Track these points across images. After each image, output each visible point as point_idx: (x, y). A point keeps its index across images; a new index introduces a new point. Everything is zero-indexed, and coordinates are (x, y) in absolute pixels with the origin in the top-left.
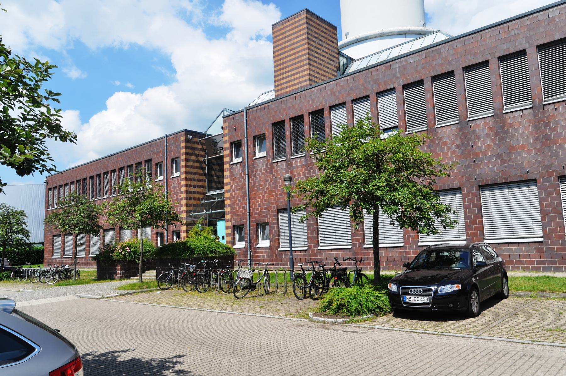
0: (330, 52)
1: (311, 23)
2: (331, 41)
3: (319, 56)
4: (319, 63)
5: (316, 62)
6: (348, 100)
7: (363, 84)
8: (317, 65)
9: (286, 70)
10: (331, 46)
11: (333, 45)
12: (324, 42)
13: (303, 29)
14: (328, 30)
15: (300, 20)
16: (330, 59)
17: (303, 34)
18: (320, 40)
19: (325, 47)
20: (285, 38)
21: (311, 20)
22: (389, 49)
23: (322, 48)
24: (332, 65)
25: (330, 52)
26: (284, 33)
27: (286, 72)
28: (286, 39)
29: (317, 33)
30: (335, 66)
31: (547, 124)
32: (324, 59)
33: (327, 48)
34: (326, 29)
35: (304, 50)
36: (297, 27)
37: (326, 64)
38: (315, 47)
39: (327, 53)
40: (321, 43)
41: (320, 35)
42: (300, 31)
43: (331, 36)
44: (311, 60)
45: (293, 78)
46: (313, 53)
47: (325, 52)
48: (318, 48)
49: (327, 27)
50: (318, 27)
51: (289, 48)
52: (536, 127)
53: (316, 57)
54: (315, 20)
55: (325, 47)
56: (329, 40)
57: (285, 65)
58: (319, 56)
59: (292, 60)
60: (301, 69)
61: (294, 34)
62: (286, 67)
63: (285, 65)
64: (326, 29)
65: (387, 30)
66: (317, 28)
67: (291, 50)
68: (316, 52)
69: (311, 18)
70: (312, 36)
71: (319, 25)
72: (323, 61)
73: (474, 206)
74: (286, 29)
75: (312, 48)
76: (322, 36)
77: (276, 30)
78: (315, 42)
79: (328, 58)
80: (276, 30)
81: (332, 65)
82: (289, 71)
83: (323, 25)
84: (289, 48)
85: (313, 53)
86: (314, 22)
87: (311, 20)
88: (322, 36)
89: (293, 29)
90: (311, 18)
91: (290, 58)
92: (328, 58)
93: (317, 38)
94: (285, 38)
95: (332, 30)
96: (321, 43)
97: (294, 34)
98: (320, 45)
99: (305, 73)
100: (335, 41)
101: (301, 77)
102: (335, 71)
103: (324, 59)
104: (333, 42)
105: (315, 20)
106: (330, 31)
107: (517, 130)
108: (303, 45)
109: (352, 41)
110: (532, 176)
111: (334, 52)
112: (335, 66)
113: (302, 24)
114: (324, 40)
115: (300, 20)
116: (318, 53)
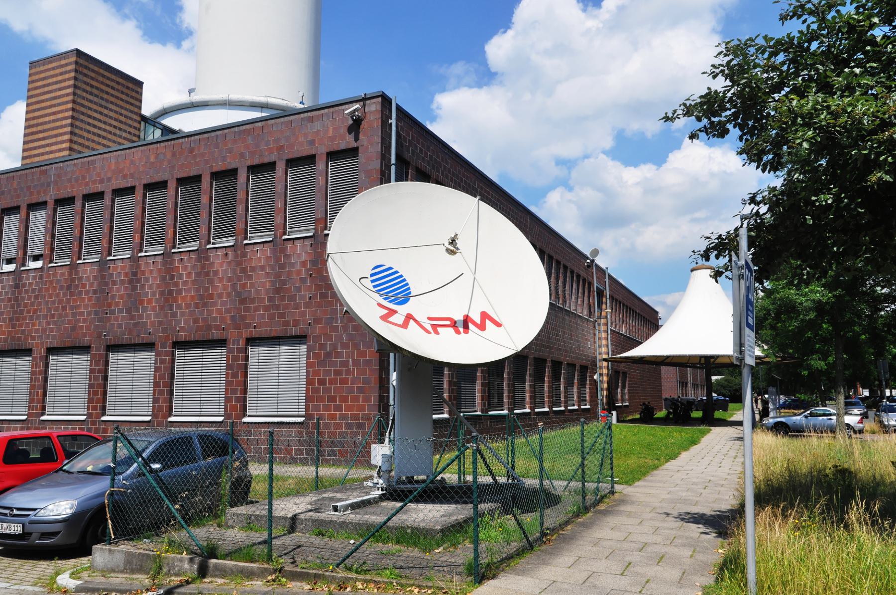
0: (122, 118)
1: (85, 71)
2: (127, 102)
3: (96, 123)
7: (15, 190)
8: (90, 136)
9: (41, 135)
10: (127, 110)
11: (132, 108)
12: (112, 103)
13: (69, 79)
14: (123, 85)
15: (66, 65)
16: (120, 129)
17: (69, 87)
18: (102, 98)
19: (111, 110)
20: (44, 86)
21: (86, 67)
23: (106, 112)
25: (122, 118)
26: (44, 79)
27: (39, 140)
28: (46, 89)
29: (97, 88)
31: (172, 277)
32: (108, 128)
33: (116, 112)
34: (118, 83)
35: (67, 110)
36: (61, 74)
37: (110, 136)
38: (90, 109)
39: (116, 120)
40: (103, 103)
41: (102, 91)
42: (65, 80)
43: (127, 95)
44: (77, 127)
45: (47, 149)
47: (111, 118)
48: (96, 111)
49: (121, 80)
50: (101, 79)
51: (48, 103)
52: (163, 278)
53: (89, 124)
54: (96, 69)
55: (111, 110)
56: (122, 100)
57: (40, 128)
58: (96, 123)
59: (49, 122)
60: (60, 139)
61: (56, 83)
62: (41, 132)
63: (40, 128)
64: (118, 83)
65: (235, 97)
66: (97, 81)
67: (51, 107)
68: (89, 116)
69: (86, 63)
70: (84, 90)
71: (103, 76)
72: (105, 130)
73: (100, 371)
74: (48, 74)
75: (82, 109)
76: (107, 93)
77: (33, 71)
78: (91, 101)
79: (115, 127)
80: (33, 71)
82: (44, 139)
83: (113, 77)
84: (48, 103)
85: (82, 117)
86: (93, 71)
87: (86, 67)
88: (107, 93)
89: (56, 75)
90: (86, 63)
91: (47, 119)
92: (115, 127)
93: (96, 96)
94: (44, 86)
95: (130, 85)
96: (103, 103)
97: (56, 83)
98: (101, 106)
99: (64, 146)
100: (137, 103)
101: (60, 149)
103: (108, 128)
104: (132, 104)
105: (96, 69)
106: (128, 88)
107: (147, 279)
108: (67, 103)
109: (185, 104)
110: (152, 339)
111: (131, 119)
113: (70, 72)
114: (112, 99)
115: (66, 65)
116: (94, 118)
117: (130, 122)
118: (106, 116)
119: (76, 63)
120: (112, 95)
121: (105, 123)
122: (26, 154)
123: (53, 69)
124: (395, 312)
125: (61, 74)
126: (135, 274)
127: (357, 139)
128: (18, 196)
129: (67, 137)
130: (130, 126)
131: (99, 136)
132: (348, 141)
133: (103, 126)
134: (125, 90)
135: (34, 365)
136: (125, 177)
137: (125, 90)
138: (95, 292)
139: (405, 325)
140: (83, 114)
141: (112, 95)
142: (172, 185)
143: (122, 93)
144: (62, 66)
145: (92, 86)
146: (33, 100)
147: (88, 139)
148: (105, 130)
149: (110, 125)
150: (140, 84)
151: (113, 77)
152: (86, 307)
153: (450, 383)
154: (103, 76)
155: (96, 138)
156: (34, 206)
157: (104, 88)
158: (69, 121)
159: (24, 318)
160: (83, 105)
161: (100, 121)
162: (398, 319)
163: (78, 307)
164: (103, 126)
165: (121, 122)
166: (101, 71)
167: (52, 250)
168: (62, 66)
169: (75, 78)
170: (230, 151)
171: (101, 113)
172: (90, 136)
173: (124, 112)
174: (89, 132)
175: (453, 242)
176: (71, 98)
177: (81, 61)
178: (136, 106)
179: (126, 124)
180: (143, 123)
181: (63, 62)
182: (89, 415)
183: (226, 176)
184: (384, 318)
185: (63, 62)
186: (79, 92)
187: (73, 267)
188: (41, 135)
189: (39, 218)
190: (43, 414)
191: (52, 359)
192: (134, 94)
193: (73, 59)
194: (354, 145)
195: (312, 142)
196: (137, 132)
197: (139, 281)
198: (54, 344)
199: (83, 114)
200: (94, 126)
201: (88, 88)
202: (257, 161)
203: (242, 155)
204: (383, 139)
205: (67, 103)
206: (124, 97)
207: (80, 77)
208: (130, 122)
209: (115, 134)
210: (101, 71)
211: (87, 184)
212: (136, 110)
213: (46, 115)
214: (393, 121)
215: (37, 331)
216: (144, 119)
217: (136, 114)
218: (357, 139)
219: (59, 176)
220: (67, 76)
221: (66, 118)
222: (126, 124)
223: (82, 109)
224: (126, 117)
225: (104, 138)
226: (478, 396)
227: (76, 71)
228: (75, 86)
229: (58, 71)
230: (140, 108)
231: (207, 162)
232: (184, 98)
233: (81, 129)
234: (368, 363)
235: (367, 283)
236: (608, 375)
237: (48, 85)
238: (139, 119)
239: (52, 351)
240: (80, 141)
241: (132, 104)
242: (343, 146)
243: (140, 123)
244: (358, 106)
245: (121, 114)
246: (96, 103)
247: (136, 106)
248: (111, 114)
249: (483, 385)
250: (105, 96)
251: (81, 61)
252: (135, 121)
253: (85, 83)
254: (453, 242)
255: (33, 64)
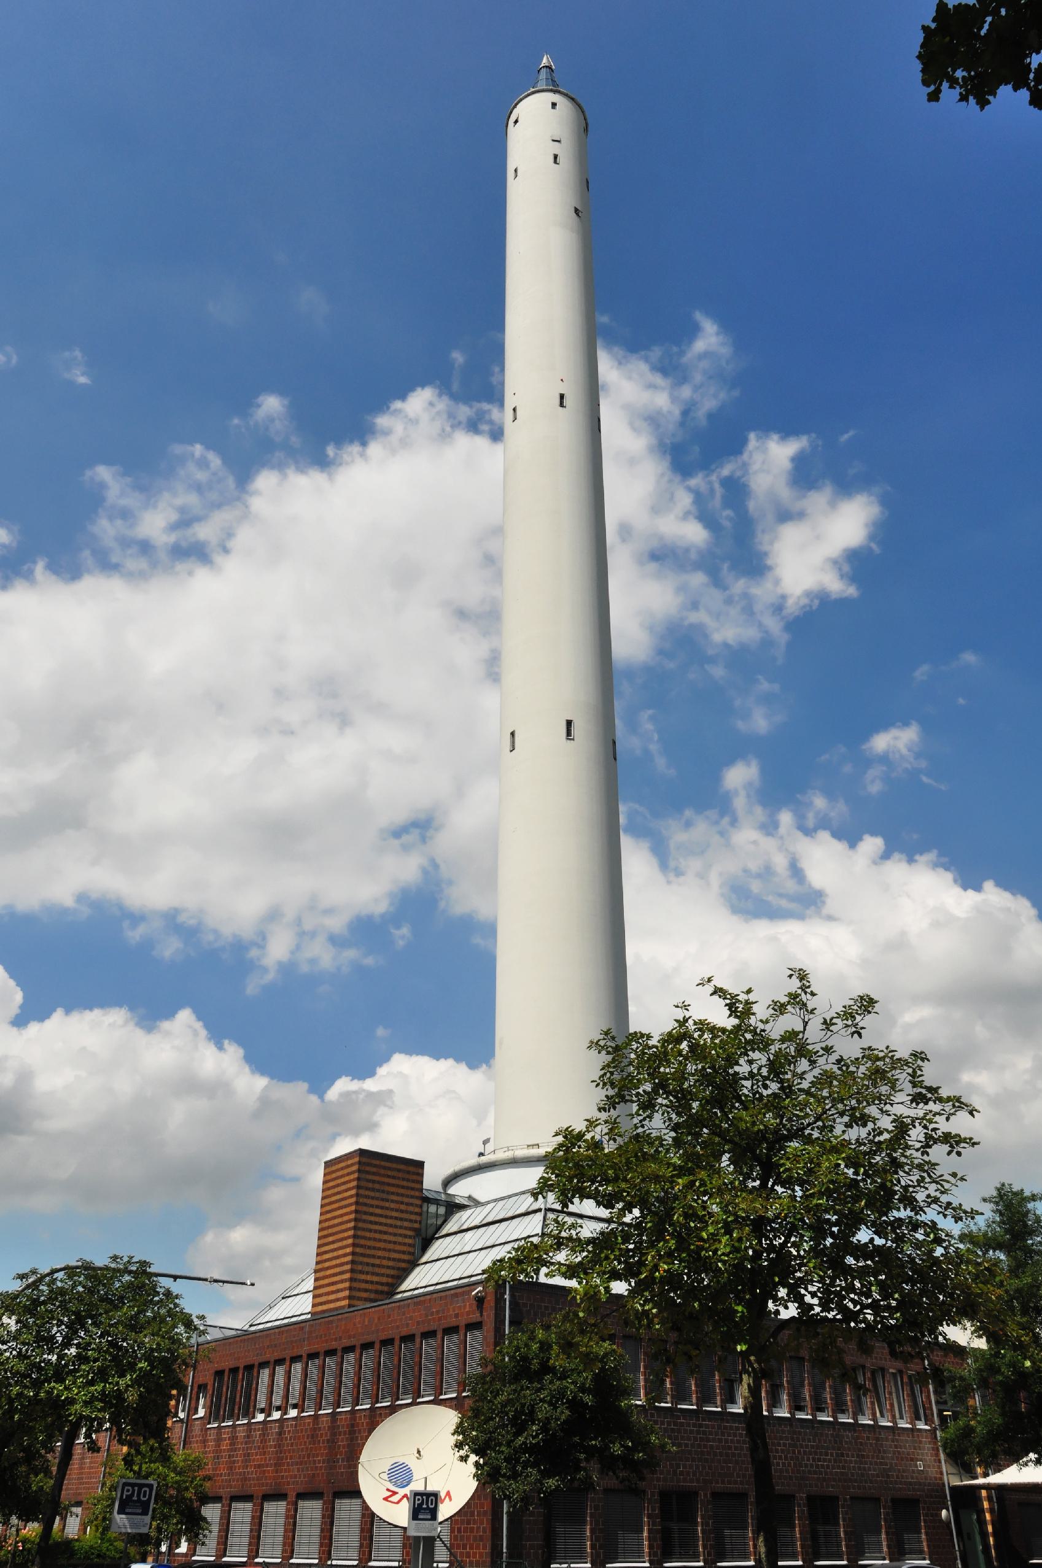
0: (403, 1207)
1: (368, 1168)
3: (377, 1219)
4: (376, 1231)
5: (370, 1231)
6: (272, 1360)
8: (372, 1235)
9: (331, 1239)
10: (407, 1196)
11: (412, 1193)
12: (393, 1193)
13: (353, 1180)
15: (352, 1165)
16: (401, 1219)
18: (383, 1192)
19: (392, 1201)
22: (495, 1200)
23: (387, 1204)
24: (406, 1228)
25: (403, 1207)
29: (379, 1182)
30: (410, 1229)
32: (389, 1221)
33: (397, 1202)
34: (399, 1170)
35: (351, 1213)
36: (348, 1174)
38: (372, 1206)
39: (397, 1210)
40: (385, 1196)
41: (383, 1183)
43: (408, 1180)
45: (335, 1254)
46: (364, 1217)
47: (392, 1210)
48: (377, 1207)
49: (402, 1167)
50: (382, 1171)
53: (371, 1222)
55: (392, 1201)
56: (403, 1187)
58: (377, 1219)
60: (345, 1243)
63: (330, 1231)
64: (399, 1170)
68: (371, 1214)
70: (367, 1189)
72: (386, 1225)
75: (365, 1209)
76: (389, 1184)
81: (406, 1228)
83: (394, 1166)
85: (364, 1217)
86: (375, 1166)
88: (389, 1184)
92: (396, 1218)
93: (378, 1191)
95: (411, 1169)
96: (385, 1196)
98: (383, 1200)
99: (348, 1250)
100: (417, 1186)
102: (410, 1237)
103: (389, 1221)
104: (413, 1189)
106: (408, 1172)
107: (360, 1431)
111: (412, 1204)
112: (410, 1229)
115: (352, 1165)
117: (411, 1209)
118: (387, 1208)
119: (360, 1163)
120: (393, 1185)
121: (386, 1217)
122: (319, 1258)
123: (342, 1169)
124: (395, 1493)
125: (348, 1174)
126: (353, 1426)
127: (481, 1315)
128: (285, 1349)
129: (350, 1241)
130: (412, 1213)
131: (381, 1232)
132: (475, 1317)
133: (383, 1220)
134: (407, 1176)
135: (288, 1510)
136: (350, 1337)
137: (407, 1176)
138: (328, 1441)
139: (398, 1503)
140: (365, 1213)
141: (393, 1185)
142: (377, 1346)
143: (403, 1179)
144: (348, 1166)
145: (374, 1182)
146: (327, 1201)
147: (370, 1239)
148: (386, 1225)
149: (391, 1218)
150: (421, 1164)
151: (394, 1166)
152: (322, 1455)
153: (592, 1531)
154: (385, 1168)
155: (377, 1236)
156: (295, 1359)
157: (386, 1180)
158: (352, 1224)
159: (283, 1464)
160: (366, 1205)
161: (381, 1216)
162: (395, 1498)
163: (317, 1455)
164: (383, 1220)
165: (402, 1211)
166: (383, 1163)
167: (304, 1401)
168: (348, 1166)
169: (358, 1179)
170: (411, 1318)
171: (382, 1208)
172: (372, 1235)
173: (406, 1200)
174: (370, 1231)
175: (419, 1452)
176: (353, 1200)
177: (364, 1160)
178: (417, 1190)
179: (407, 1212)
180: (425, 1205)
181: (350, 1162)
182: (320, 1559)
183: (408, 1338)
184: (386, 1499)
185: (350, 1162)
186: (362, 1192)
187: (316, 1417)
188: (331, 1239)
189: (297, 1368)
190: (292, 1558)
191: (301, 1503)
192: (415, 1177)
193: (357, 1159)
194: (479, 1320)
195: (457, 1316)
196: (418, 1218)
197: (354, 1432)
198: (301, 1491)
199: (365, 1213)
200: (376, 1223)
201: (370, 1185)
202: (426, 1330)
203: (418, 1323)
204: (496, 1314)
205: (351, 1205)
206: (405, 1183)
207: (363, 1176)
208: (411, 1209)
209: (396, 1227)
210: (383, 1163)
211: (327, 1341)
212: (417, 1194)
213: (334, 1218)
214: (507, 1297)
215: (291, 1477)
216: (428, 1200)
217: (417, 1198)
218: (481, 1315)
219: (310, 1332)
220: (352, 1177)
221: (349, 1221)
222: (407, 1212)
223: (365, 1209)
224: (407, 1204)
225: (385, 1233)
226: (884, 1543)
227: (359, 1171)
228: (358, 1187)
229: (346, 1171)
230: (422, 1190)
231: (398, 1327)
232: (473, 1161)
233: (363, 1229)
234: (485, 1513)
235: (385, 1476)
236: (991, 1511)
237: (338, 1185)
238: (419, 1202)
239: (302, 1496)
240: (362, 1242)
241: (413, 1189)
242: (474, 1321)
243: (421, 1207)
244: (480, 1288)
245: (402, 1203)
246: (377, 1199)
247: (417, 1190)
248: (393, 1205)
249: (649, 1531)
250: (387, 1188)
251: (364, 1160)
252: (417, 1205)
253: (368, 1181)
254: (419, 1452)
255: (328, 1164)
